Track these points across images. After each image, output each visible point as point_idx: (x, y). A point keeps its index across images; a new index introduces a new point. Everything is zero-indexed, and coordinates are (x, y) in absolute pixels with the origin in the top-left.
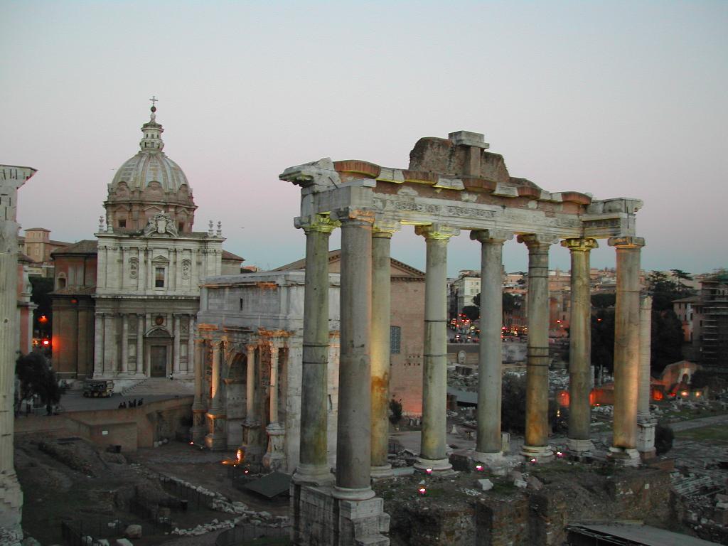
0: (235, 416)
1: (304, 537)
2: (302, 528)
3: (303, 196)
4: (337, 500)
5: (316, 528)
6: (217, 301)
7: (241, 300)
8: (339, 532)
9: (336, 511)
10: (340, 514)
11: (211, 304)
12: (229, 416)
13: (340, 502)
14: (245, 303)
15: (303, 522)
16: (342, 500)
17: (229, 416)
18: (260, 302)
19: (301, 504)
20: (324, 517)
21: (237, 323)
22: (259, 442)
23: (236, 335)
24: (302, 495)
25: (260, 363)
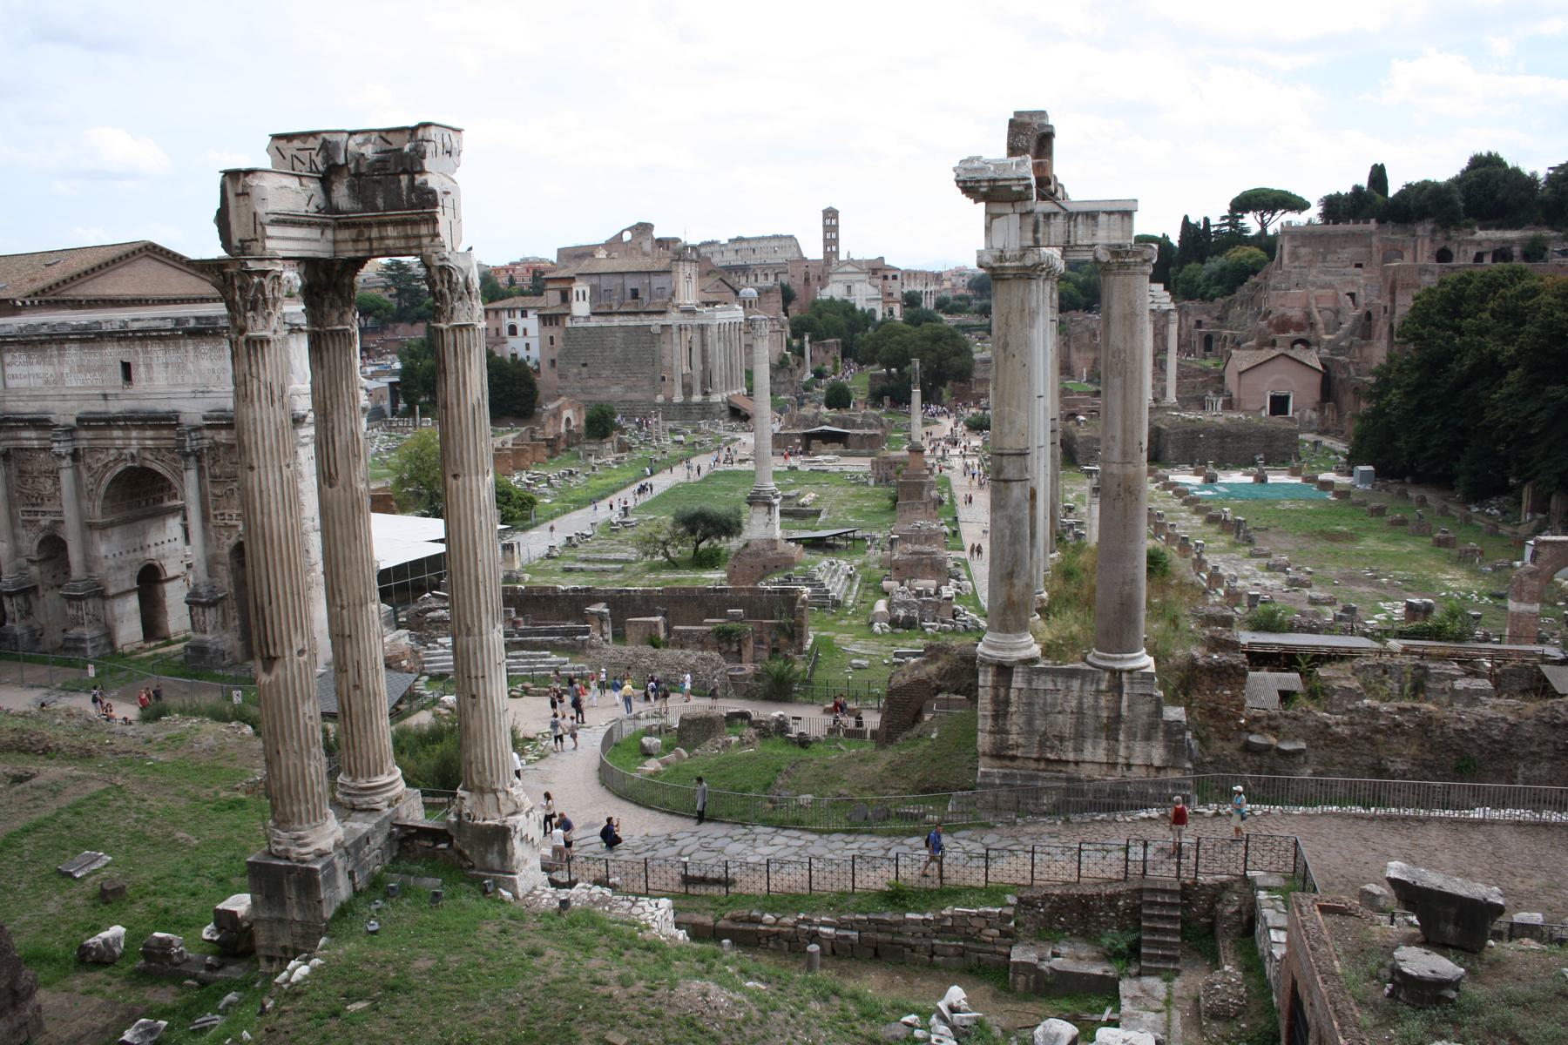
0: (121, 589)
1: (1021, 741)
2: (1014, 729)
3: (991, 217)
4: (1116, 674)
5: (1065, 723)
6: (37, 369)
7: (126, 367)
8: (1119, 715)
9: (1116, 688)
10: (1126, 690)
11: (14, 377)
12: (112, 591)
13: (1124, 676)
14: (139, 373)
15: (1015, 723)
16: (1130, 671)
17: (112, 591)
18: (191, 366)
19: (1013, 695)
20: (1080, 703)
21: (115, 407)
22: (224, 625)
23: (117, 433)
24: (1018, 681)
25: (208, 479)
